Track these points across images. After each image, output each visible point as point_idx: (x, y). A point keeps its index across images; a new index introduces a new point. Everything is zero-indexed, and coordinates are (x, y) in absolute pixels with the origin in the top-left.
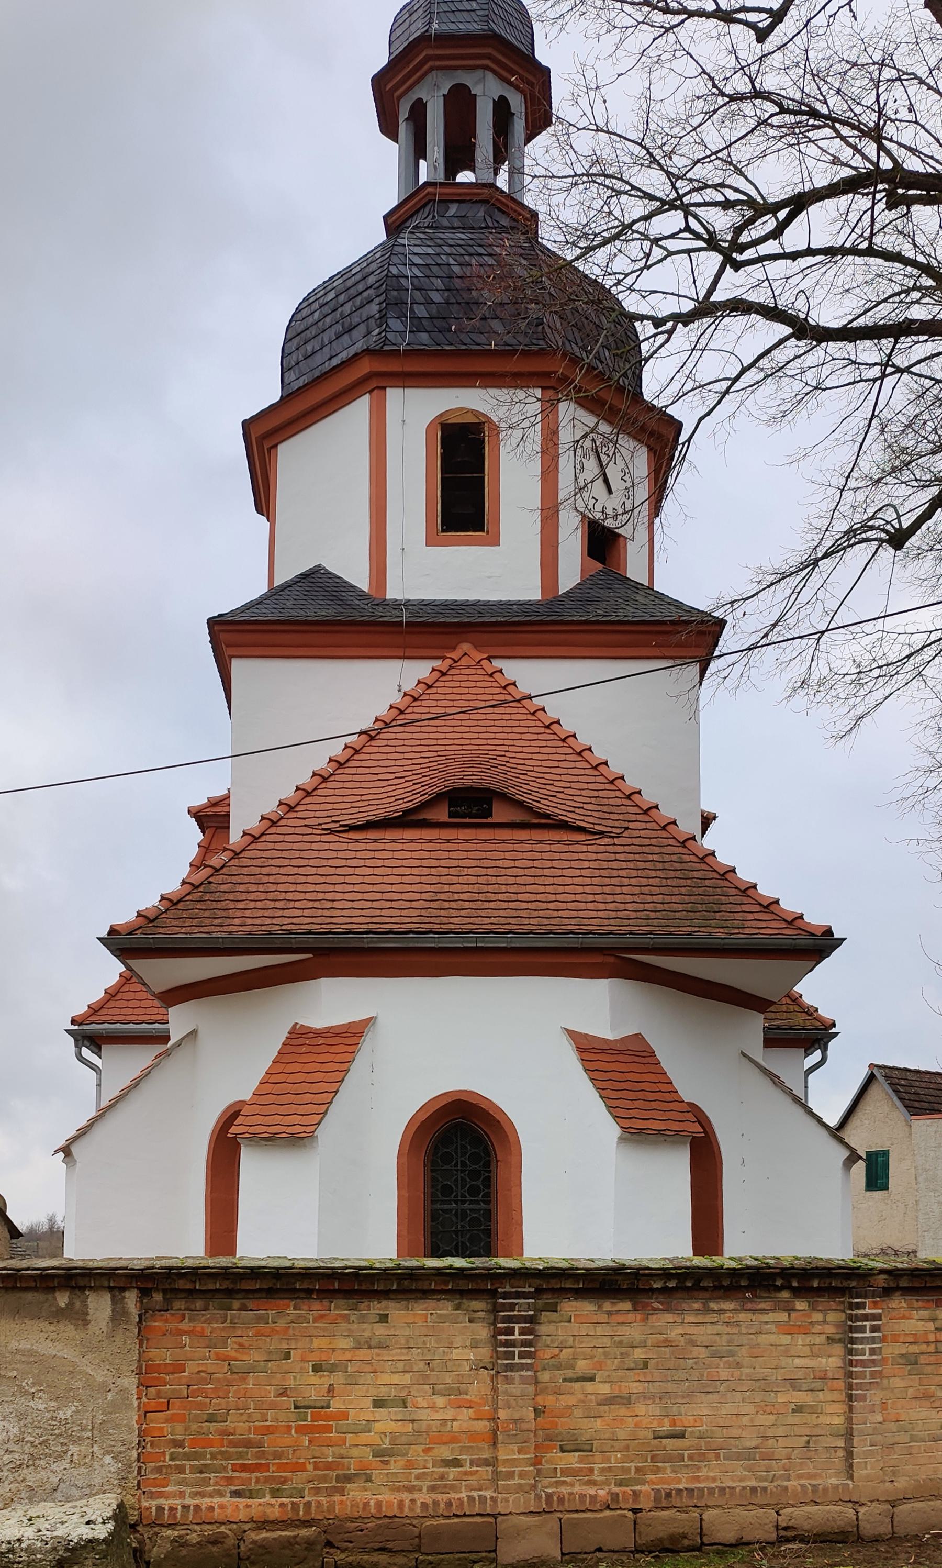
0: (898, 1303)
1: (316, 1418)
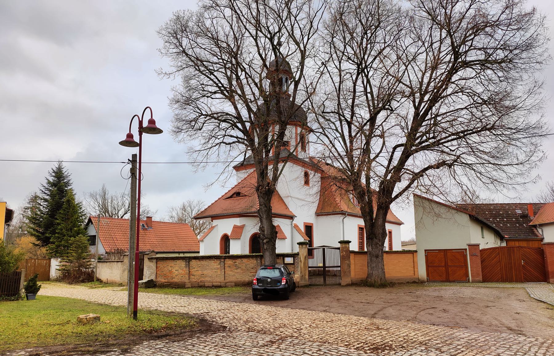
0: (227, 260)
1: (171, 272)
